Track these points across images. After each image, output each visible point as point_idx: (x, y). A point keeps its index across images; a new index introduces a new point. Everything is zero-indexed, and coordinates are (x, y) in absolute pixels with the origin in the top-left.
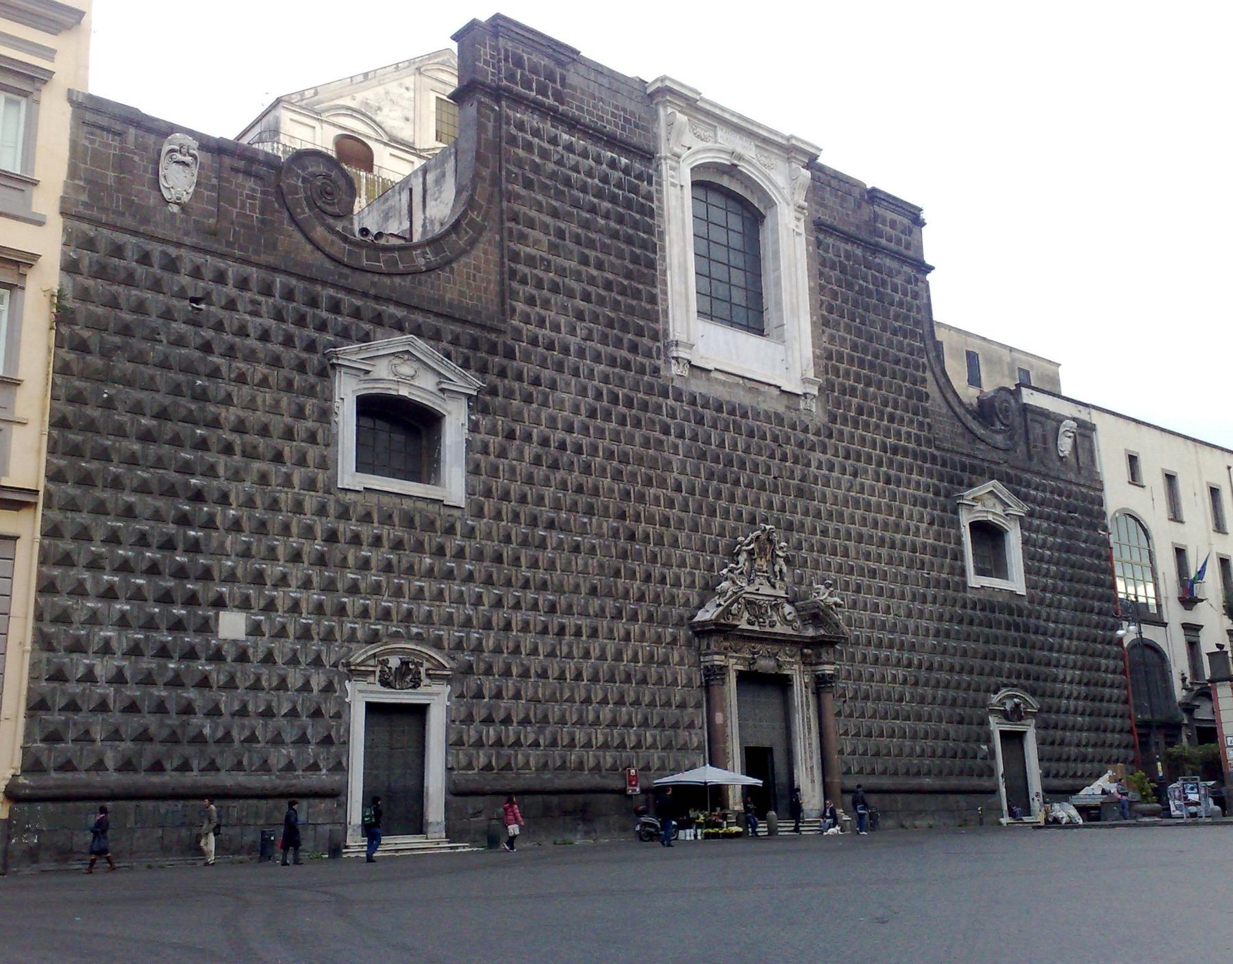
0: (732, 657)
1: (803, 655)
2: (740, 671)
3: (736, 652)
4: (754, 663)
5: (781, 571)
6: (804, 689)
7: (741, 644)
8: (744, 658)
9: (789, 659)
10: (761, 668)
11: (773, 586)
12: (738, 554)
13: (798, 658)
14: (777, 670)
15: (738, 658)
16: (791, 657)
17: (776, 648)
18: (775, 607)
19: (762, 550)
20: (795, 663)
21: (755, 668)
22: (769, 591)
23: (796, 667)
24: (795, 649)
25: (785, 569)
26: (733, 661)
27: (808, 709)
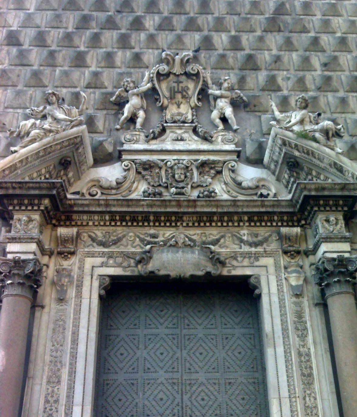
0: (92, 255)
1: (282, 238)
2: (114, 278)
3: (103, 244)
6: (289, 301)
7: (120, 231)
8: (127, 256)
9: (246, 249)
11: (206, 139)
13: (274, 246)
14: (210, 268)
15: (110, 256)
16: (256, 245)
17: (213, 233)
20: (266, 254)
21: (151, 267)
22: (195, 144)
23: (269, 261)
24: (263, 232)
26: (89, 262)
27: (303, 337)
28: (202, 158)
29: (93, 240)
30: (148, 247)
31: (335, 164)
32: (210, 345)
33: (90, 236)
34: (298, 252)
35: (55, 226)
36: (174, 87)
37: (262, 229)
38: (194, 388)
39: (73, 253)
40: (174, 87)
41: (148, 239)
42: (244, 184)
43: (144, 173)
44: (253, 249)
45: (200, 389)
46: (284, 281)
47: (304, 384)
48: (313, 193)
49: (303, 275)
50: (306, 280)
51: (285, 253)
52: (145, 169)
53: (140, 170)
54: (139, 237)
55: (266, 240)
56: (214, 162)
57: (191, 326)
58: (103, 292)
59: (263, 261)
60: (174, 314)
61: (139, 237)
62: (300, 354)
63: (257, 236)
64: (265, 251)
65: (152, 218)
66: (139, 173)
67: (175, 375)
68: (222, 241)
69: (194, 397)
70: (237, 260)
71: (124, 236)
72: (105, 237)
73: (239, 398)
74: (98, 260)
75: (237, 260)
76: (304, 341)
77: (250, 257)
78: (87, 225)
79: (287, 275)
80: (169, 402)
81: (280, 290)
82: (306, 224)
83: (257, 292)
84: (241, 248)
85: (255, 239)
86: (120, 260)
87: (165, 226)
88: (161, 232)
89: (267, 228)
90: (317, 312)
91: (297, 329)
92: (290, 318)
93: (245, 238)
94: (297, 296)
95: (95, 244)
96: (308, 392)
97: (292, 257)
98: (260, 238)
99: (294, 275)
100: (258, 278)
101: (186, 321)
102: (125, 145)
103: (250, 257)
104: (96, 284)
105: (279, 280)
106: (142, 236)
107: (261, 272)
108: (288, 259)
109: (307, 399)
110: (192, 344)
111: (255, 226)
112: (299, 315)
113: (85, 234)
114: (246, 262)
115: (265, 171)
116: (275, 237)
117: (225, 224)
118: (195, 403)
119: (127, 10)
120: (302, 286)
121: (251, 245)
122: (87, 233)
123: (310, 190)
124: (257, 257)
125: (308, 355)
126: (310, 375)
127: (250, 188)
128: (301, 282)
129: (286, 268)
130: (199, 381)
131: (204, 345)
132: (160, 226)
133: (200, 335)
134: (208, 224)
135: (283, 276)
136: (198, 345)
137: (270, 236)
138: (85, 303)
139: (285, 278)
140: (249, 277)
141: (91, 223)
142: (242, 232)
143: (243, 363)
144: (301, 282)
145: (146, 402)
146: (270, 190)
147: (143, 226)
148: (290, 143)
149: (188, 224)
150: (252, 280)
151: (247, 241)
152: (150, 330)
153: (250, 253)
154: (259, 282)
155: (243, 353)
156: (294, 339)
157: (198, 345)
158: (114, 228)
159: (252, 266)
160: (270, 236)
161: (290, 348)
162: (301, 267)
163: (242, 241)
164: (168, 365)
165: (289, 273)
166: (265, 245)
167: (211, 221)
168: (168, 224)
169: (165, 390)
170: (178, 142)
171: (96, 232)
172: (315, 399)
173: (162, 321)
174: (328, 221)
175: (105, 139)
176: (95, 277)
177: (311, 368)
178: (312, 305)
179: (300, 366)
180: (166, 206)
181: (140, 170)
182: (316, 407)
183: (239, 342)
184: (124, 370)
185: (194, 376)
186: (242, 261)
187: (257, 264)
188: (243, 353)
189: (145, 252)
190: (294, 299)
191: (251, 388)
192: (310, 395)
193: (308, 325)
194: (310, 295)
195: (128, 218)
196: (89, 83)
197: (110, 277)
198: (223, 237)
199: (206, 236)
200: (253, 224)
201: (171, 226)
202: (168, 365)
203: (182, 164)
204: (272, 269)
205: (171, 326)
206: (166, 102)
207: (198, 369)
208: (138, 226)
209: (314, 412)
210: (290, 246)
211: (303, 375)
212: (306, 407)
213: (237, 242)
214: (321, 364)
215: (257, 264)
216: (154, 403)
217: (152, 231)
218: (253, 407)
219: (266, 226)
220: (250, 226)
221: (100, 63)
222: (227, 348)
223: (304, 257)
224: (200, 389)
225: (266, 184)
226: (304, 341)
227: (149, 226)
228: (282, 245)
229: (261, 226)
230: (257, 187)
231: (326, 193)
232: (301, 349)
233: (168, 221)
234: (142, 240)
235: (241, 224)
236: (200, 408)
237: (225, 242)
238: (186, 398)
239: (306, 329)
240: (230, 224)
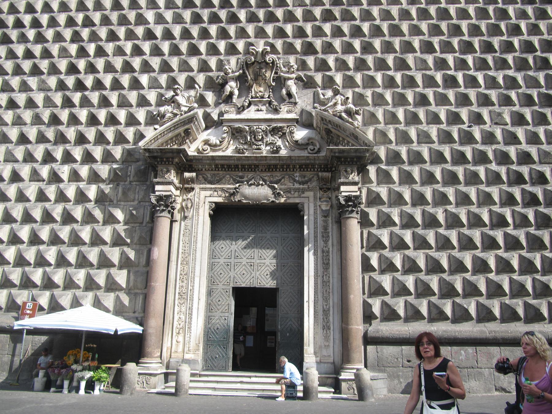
3: (211, 183)
4: (233, 194)
5: (290, 95)
9: (297, 186)
10: (246, 198)
12: (225, 83)
13: (314, 184)
15: (215, 190)
18: (274, 131)
19: (258, 78)
20: (309, 189)
23: (310, 194)
24: (309, 174)
25: (294, 89)
26: (204, 193)
27: (326, 242)
28: (274, 125)
29: (205, 180)
30: (237, 185)
31: (353, 134)
32: (274, 243)
33: (203, 177)
34: (329, 189)
35: (182, 171)
36: (257, 72)
37: (308, 172)
38: (263, 268)
39: (193, 189)
40: (257, 72)
41: (238, 179)
42: (300, 142)
43: (236, 135)
44: (301, 186)
45: (266, 269)
46: (318, 207)
47: (324, 268)
48: (337, 155)
49: (330, 203)
50: (332, 206)
51: (321, 189)
52: (237, 132)
53: (234, 132)
54: (232, 178)
55: (310, 180)
56: (281, 127)
57: (263, 232)
58: (212, 212)
59: (307, 194)
60: (254, 224)
61: (232, 178)
62: (323, 251)
63: (304, 177)
64: (309, 188)
65: (240, 167)
66: (233, 134)
67: (252, 261)
68: (283, 180)
69: (263, 272)
70: (291, 193)
71: (224, 177)
72: (212, 177)
73: (289, 274)
74: (208, 193)
75: (291, 193)
76: (326, 244)
77: (299, 192)
78: (202, 170)
79: (320, 203)
80: (248, 276)
81: (315, 213)
82: (335, 170)
83: (302, 213)
84: (294, 185)
85: (303, 179)
86: (220, 193)
87: (248, 171)
88: (246, 175)
89: (311, 172)
90: (335, 227)
91: (323, 236)
92: (320, 230)
93: (297, 179)
94: (325, 217)
95: (206, 182)
96: (325, 273)
97: (325, 192)
98: (306, 179)
99: (325, 203)
100: (303, 204)
101: (261, 229)
102: (225, 115)
103: (299, 192)
104: (207, 207)
105: (315, 206)
106: (234, 177)
107: (305, 201)
108: (321, 193)
109: (325, 277)
110: (263, 243)
111: (304, 171)
112: (325, 228)
113: (201, 176)
114: (296, 194)
115: (314, 131)
116: (315, 178)
117: (285, 170)
118: (262, 276)
119: (228, 6)
120: (329, 210)
121: (300, 184)
122: (201, 175)
123: (335, 153)
124: (303, 191)
125: (328, 252)
126: (328, 264)
127: (302, 145)
128: (328, 208)
129: (320, 199)
130: (266, 264)
131: (270, 243)
132: (245, 171)
133: (268, 237)
134: (274, 170)
135: (318, 204)
136: (267, 243)
137: (313, 177)
138: (201, 218)
139: (319, 206)
140: (298, 203)
141: (204, 170)
142: (296, 175)
143: (292, 254)
144: (328, 208)
145: (236, 275)
146: (316, 146)
147: (235, 171)
148: (326, 120)
149: (262, 170)
150: (300, 206)
151: (298, 181)
152: (239, 234)
153: (299, 189)
154: (303, 207)
155: (293, 249)
156: (321, 243)
157: (267, 243)
158: (218, 172)
159: (299, 197)
160: (313, 177)
161: (317, 248)
162: (330, 198)
163: (295, 181)
164: (249, 254)
165: (322, 202)
166: (309, 184)
167: (276, 169)
168: (250, 170)
169: (246, 269)
170: (258, 112)
171: (207, 174)
172: (329, 277)
173: (246, 228)
174: (346, 171)
175: (212, 110)
176: (206, 203)
177: (329, 259)
178: (334, 222)
179: (323, 259)
180: (248, 160)
181: (234, 132)
182: (329, 282)
183: (291, 241)
184: (224, 257)
185: (263, 261)
186: (294, 194)
187: (303, 195)
188: (293, 249)
189: (235, 188)
190: (324, 218)
191: (296, 269)
192: (326, 275)
193: (330, 234)
194: (334, 216)
195: (225, 167)
196: (202, 68)
197: (216, 203)
198: (283, 178)
199: (273, 177)
200: (302, 170)
201: (252, 171)
202: (249, 254)
203: (261, 129)
204: (312, 199)
205: (251, 231)
206: (252, 83)
207: (266, 258)
208: (232, 171)
209: (328, 284)
210: (324, 185)
211: (324, 263)
212: (323, 282)
213: (292, 181)
214: (335, 258)
215: (303, 195)
216: (240, 276)
217: (241, 174)
218: (296, 280)
219: (311, 171)
220: (300, 170)
221: (209, 51)
222: (284, 245)
223: (333, 191)
224: (266, 269)
225: (314, 141)
226: (326, 244)
227: (238, 170)
228: (320, 184)
229: (307, 171)
230: (308, 144)
231: (345, 154)
232: (324, 249)
233: (250, 168)
234: (234, 180)
235: (295, 170)
236: (265, 279)
237: (284, 181)
238: (258, 273)
239: (328, 236)
240: (288, 170)
